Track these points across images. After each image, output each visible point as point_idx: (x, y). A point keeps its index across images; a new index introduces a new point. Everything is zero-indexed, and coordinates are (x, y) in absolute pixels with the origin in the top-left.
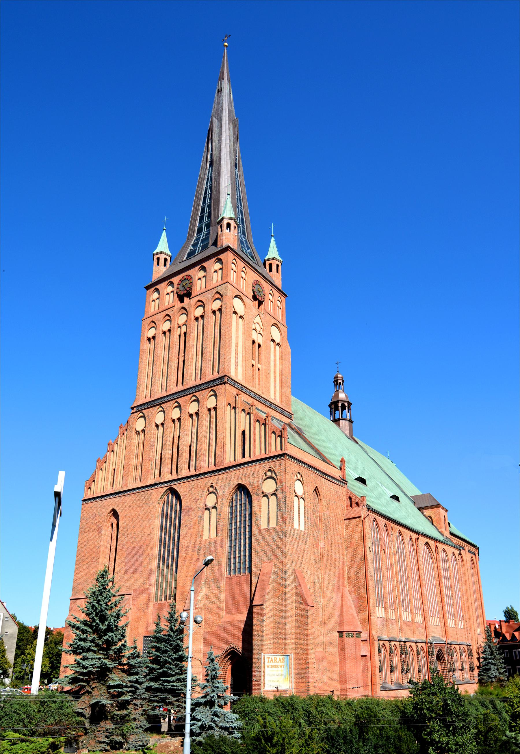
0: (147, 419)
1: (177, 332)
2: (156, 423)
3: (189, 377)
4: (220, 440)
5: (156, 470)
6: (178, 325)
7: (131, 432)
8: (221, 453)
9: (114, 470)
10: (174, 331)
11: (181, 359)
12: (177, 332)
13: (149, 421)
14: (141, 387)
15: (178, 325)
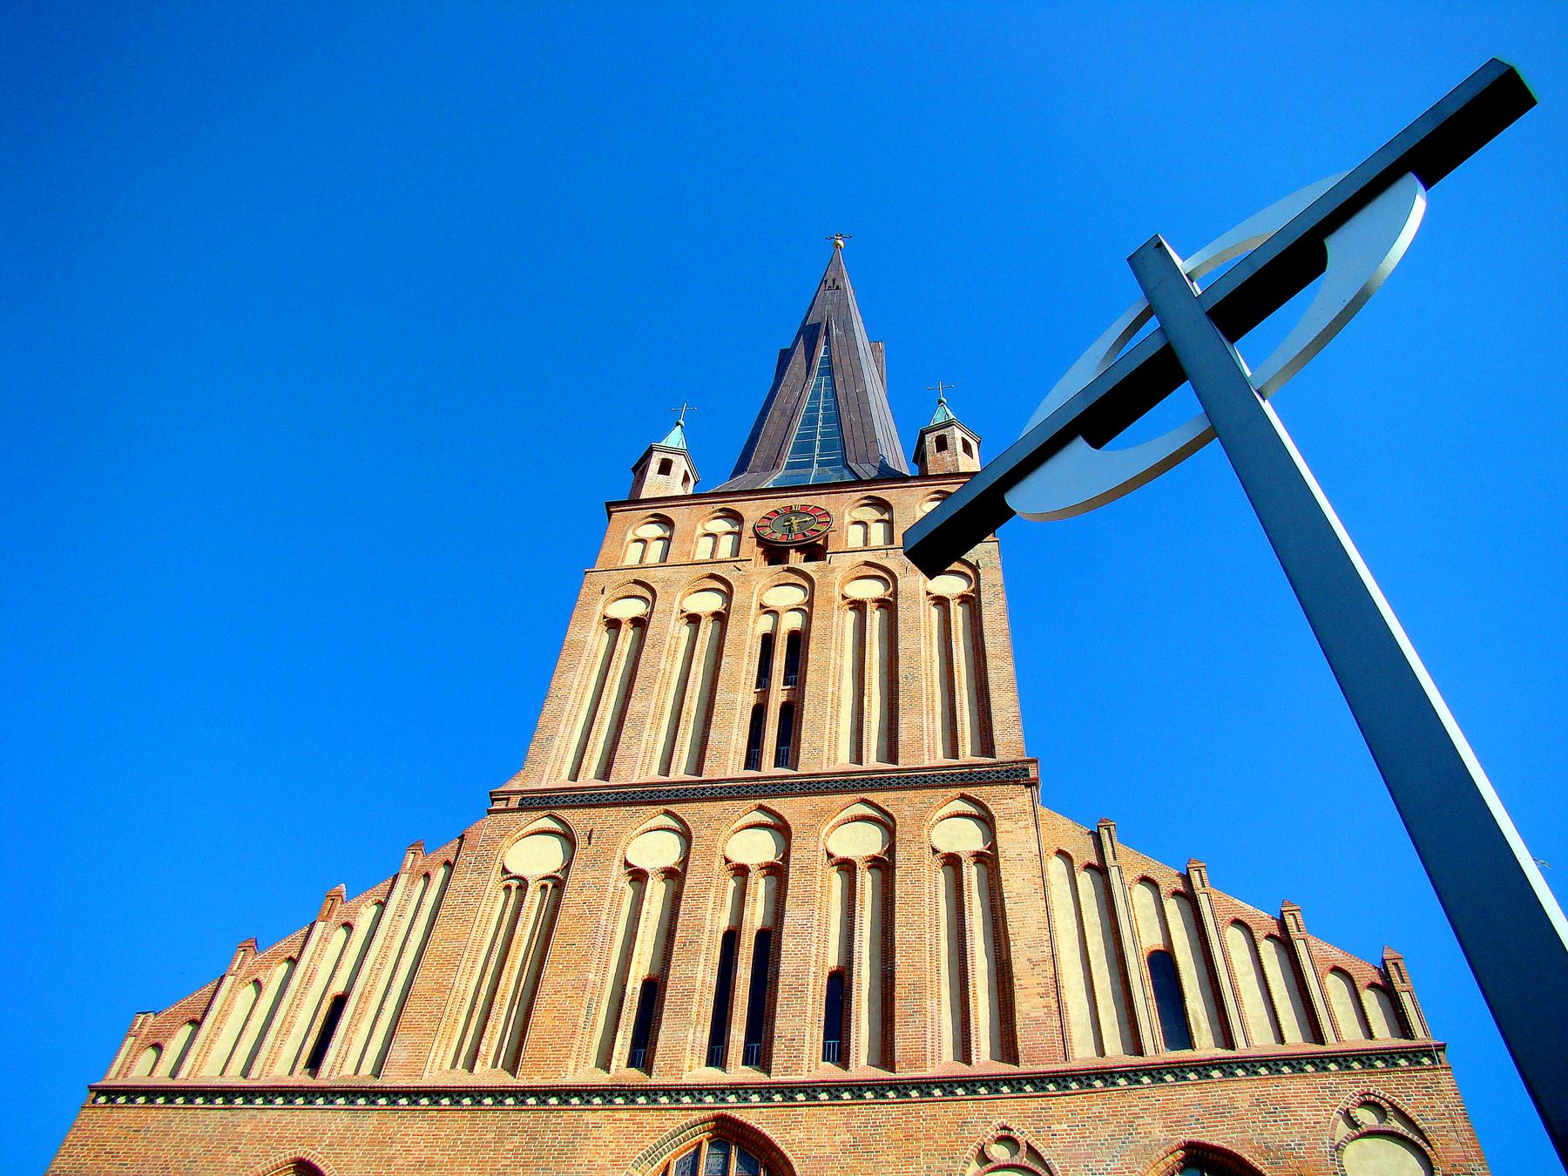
0: (581, 843)
1: (748, 632)
2: (627, 864)
3: (826, 743)
4: (1034, 964)
5: (620, 1035)
6: (762, 606)
7: (481, 868)
8: (1049, 1015)
9: (340, 1002)
10: (745, 617)
11: (778, 694)
12: (748, 632)
13: (592, 850)
14: (557, 742)
15: (762, 606)
